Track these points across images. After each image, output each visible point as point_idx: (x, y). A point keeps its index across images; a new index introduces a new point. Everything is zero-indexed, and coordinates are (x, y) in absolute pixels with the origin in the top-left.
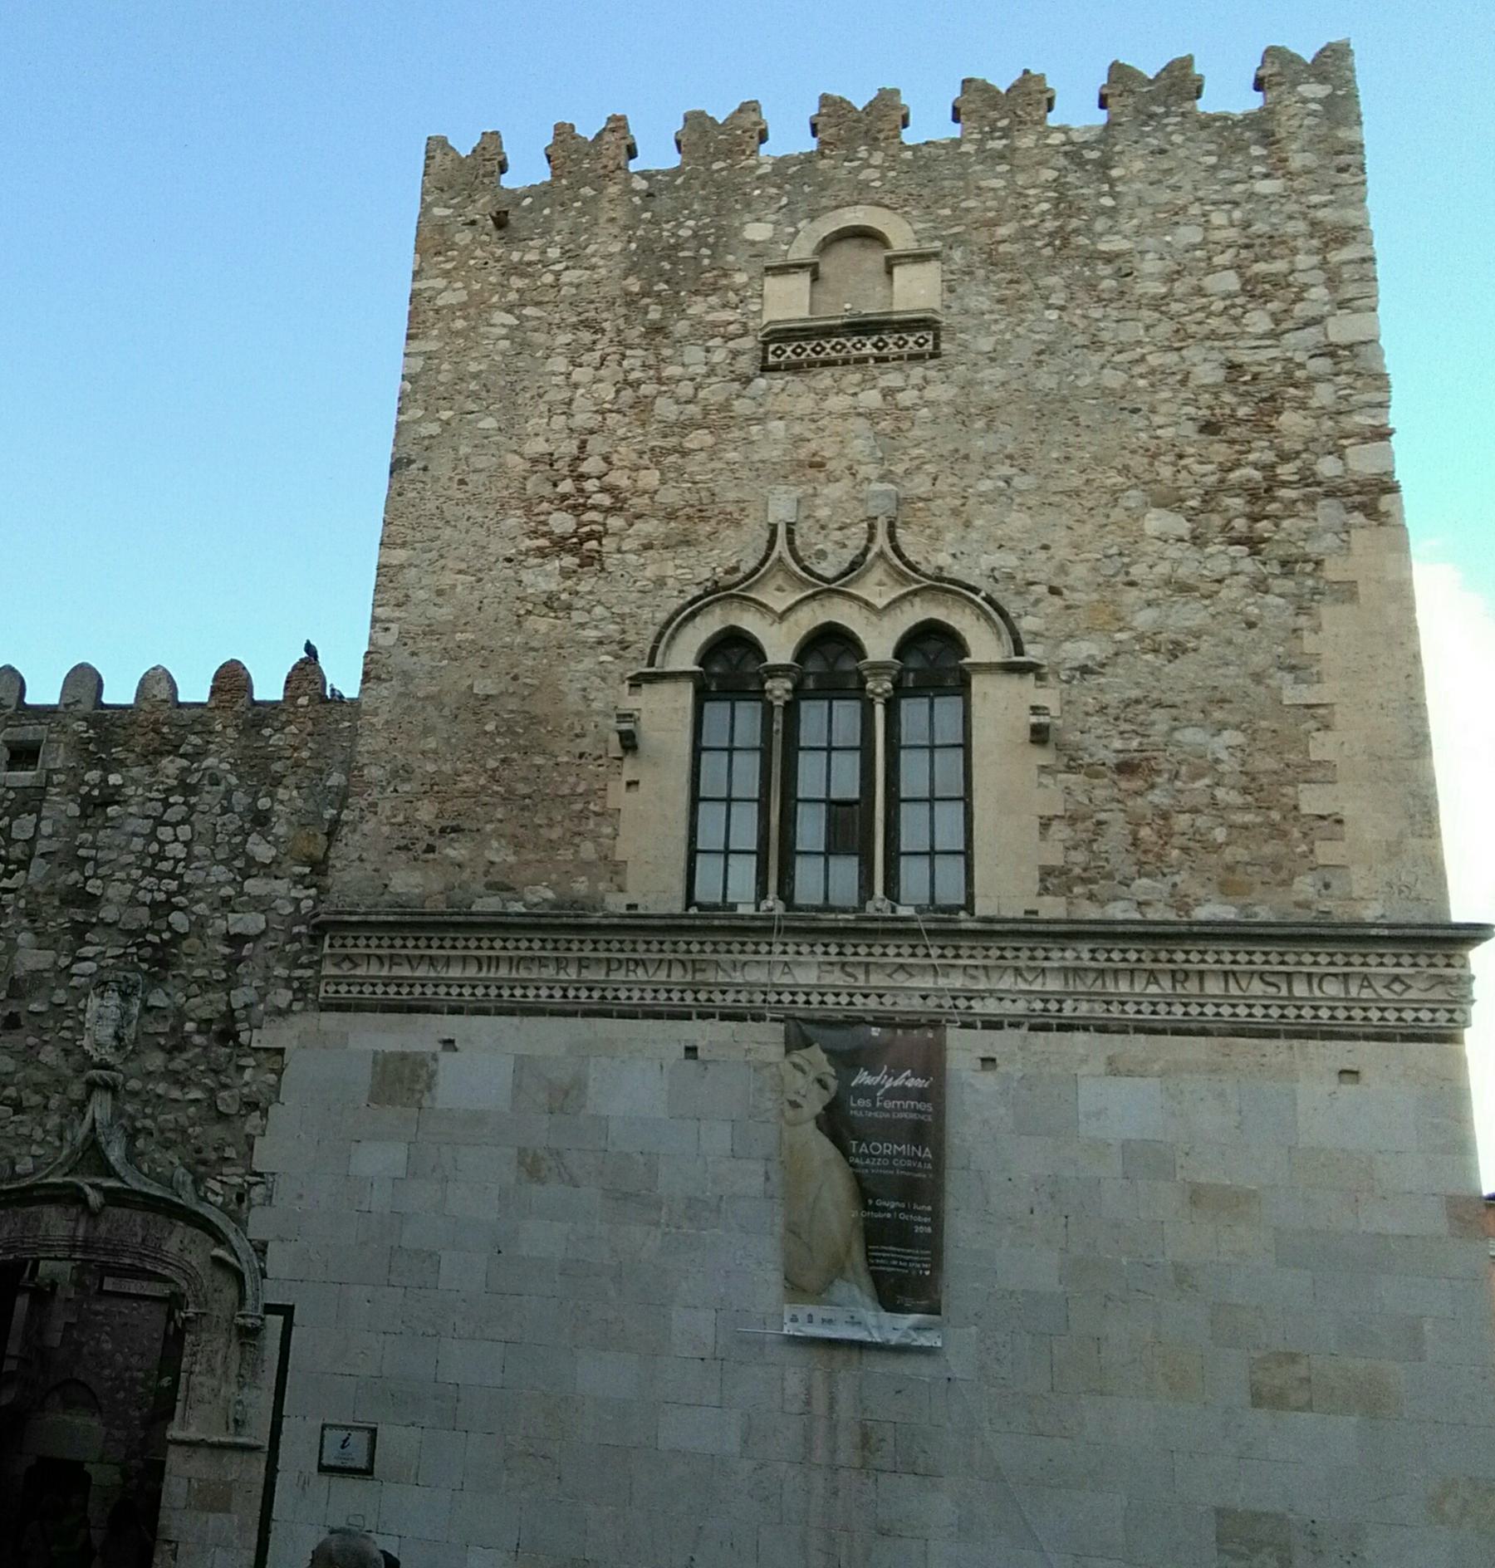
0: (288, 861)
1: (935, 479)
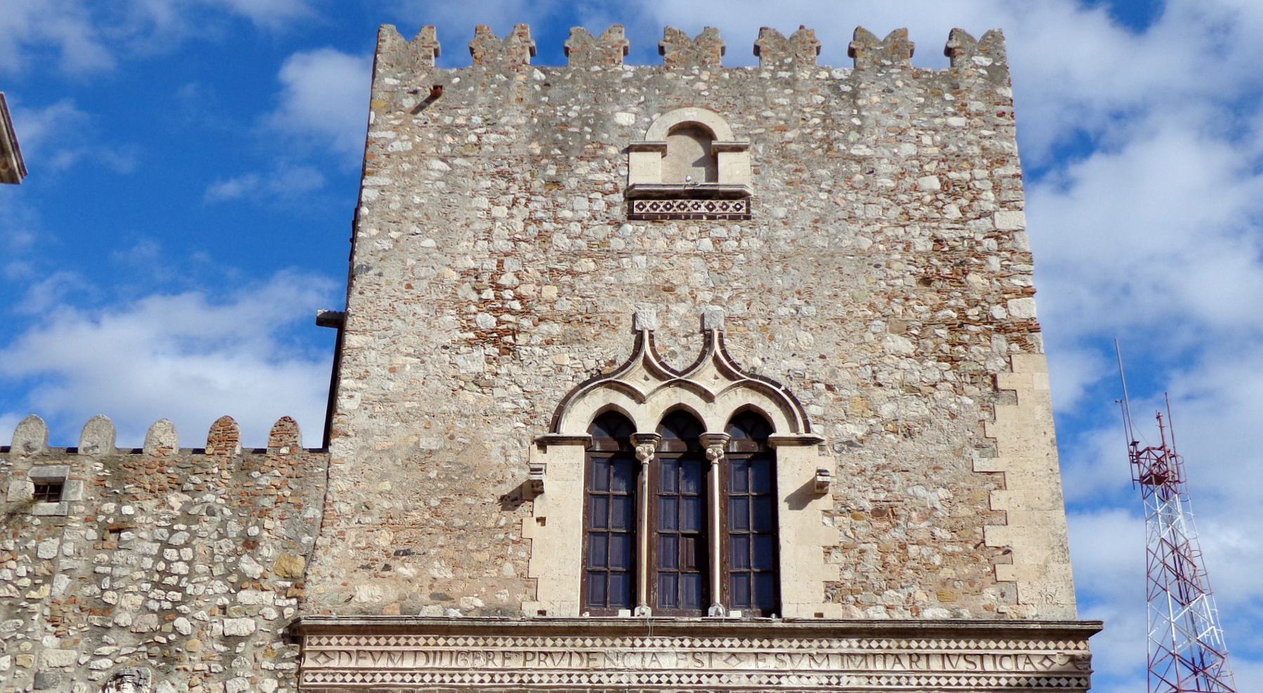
0: (272, 577)
1: (749, 305)
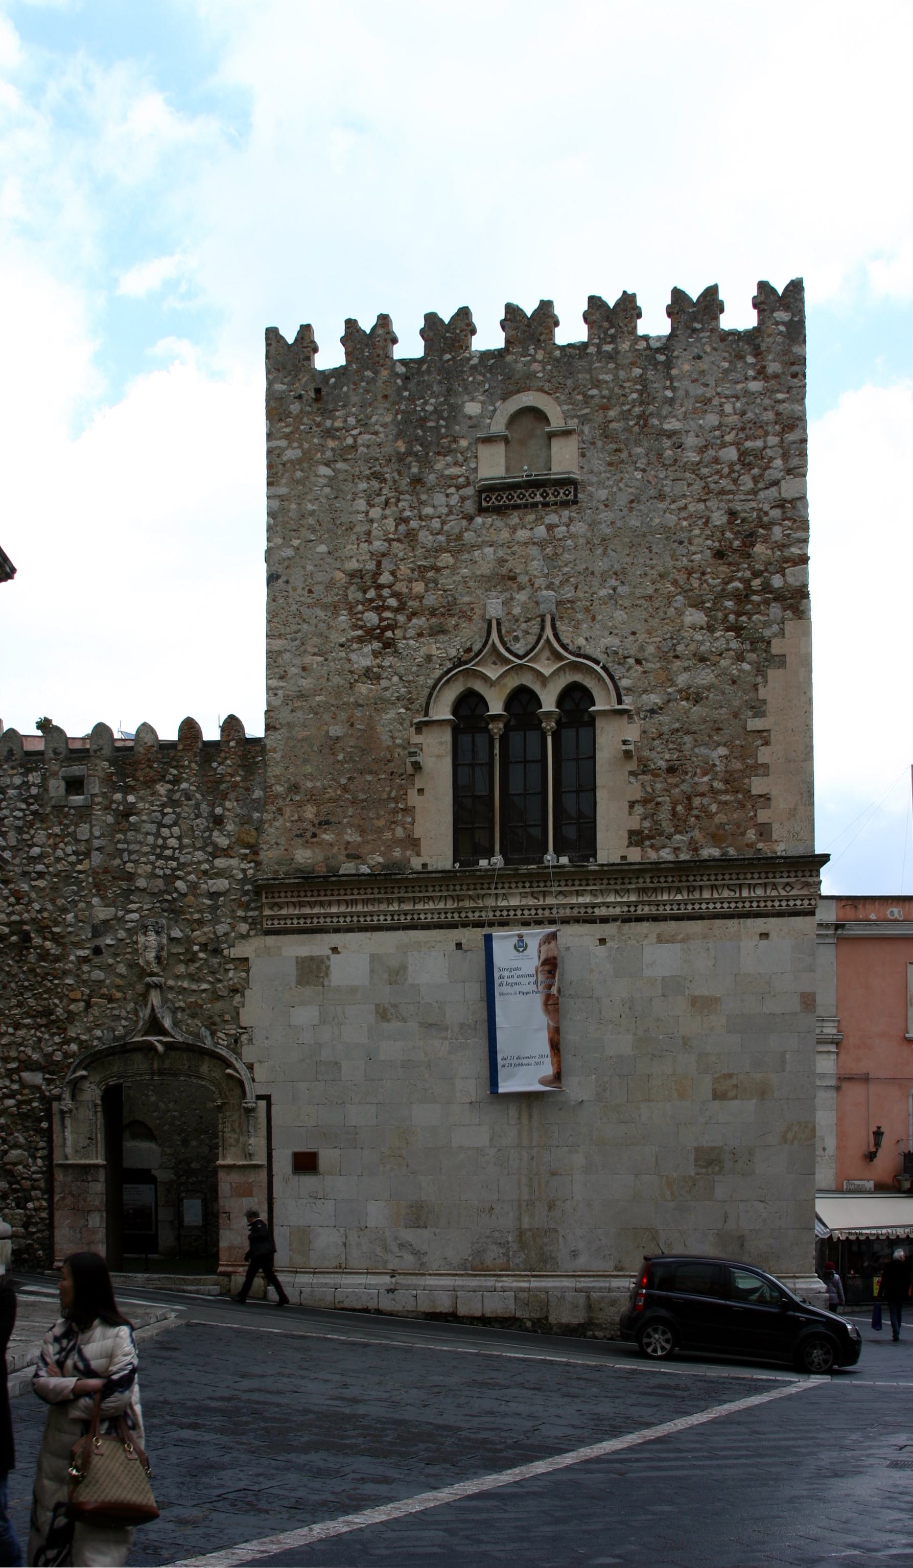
1: (576, 588)
